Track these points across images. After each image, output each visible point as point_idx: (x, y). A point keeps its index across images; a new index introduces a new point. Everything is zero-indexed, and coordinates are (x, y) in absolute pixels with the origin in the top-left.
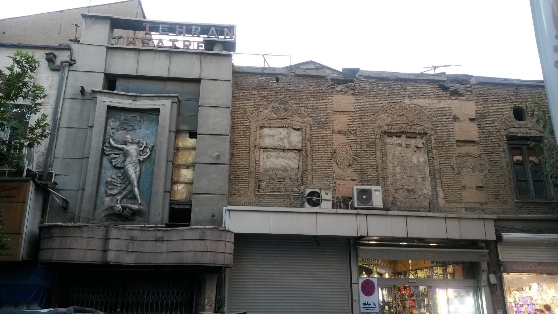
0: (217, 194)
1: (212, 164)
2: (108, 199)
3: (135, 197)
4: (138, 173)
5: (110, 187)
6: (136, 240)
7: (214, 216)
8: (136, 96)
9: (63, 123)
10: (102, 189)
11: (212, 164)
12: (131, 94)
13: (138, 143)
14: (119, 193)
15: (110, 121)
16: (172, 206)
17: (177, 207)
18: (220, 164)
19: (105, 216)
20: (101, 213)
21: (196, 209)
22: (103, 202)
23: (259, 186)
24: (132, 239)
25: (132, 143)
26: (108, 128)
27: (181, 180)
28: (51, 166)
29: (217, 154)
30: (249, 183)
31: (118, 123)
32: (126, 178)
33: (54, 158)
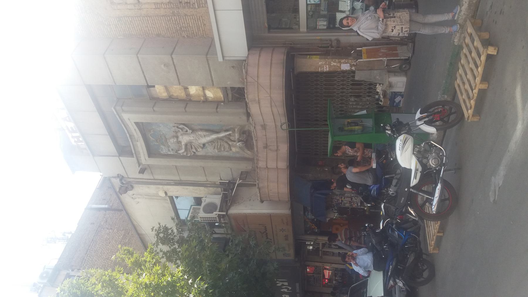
0: (208, 64)
1: (176, 70)
2: (234, 149)
3: (228, 137)
4: (205, 133)
5: (223, 149)
6: (267, 144)
7: (233, 67)
8: (130, 136)
9: (177, 178)
10: (225, 154)
11: (176, 70)
12: (130, 140)
13: (176, 132)
14: (227, 143)
15: (162, 152)
16: (230, 100)
17: (230, 96)
18: (173, 63)
19: (249, 150)
20: (248, 154)
21: (229, 83)
22: (237, 152)
23: (187, 3)
24: (266, 147)
25: (177, 137)
26: (169, 153)
27: (201, 93)
28: (215, 184)
29: (162, 66)
30: (186, 15)
31: (163, 147)
32: (212, 142)
33: (207, 181)
